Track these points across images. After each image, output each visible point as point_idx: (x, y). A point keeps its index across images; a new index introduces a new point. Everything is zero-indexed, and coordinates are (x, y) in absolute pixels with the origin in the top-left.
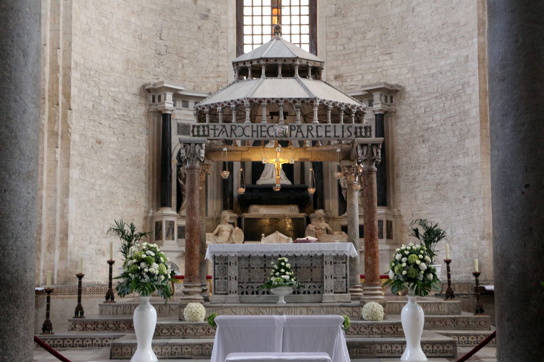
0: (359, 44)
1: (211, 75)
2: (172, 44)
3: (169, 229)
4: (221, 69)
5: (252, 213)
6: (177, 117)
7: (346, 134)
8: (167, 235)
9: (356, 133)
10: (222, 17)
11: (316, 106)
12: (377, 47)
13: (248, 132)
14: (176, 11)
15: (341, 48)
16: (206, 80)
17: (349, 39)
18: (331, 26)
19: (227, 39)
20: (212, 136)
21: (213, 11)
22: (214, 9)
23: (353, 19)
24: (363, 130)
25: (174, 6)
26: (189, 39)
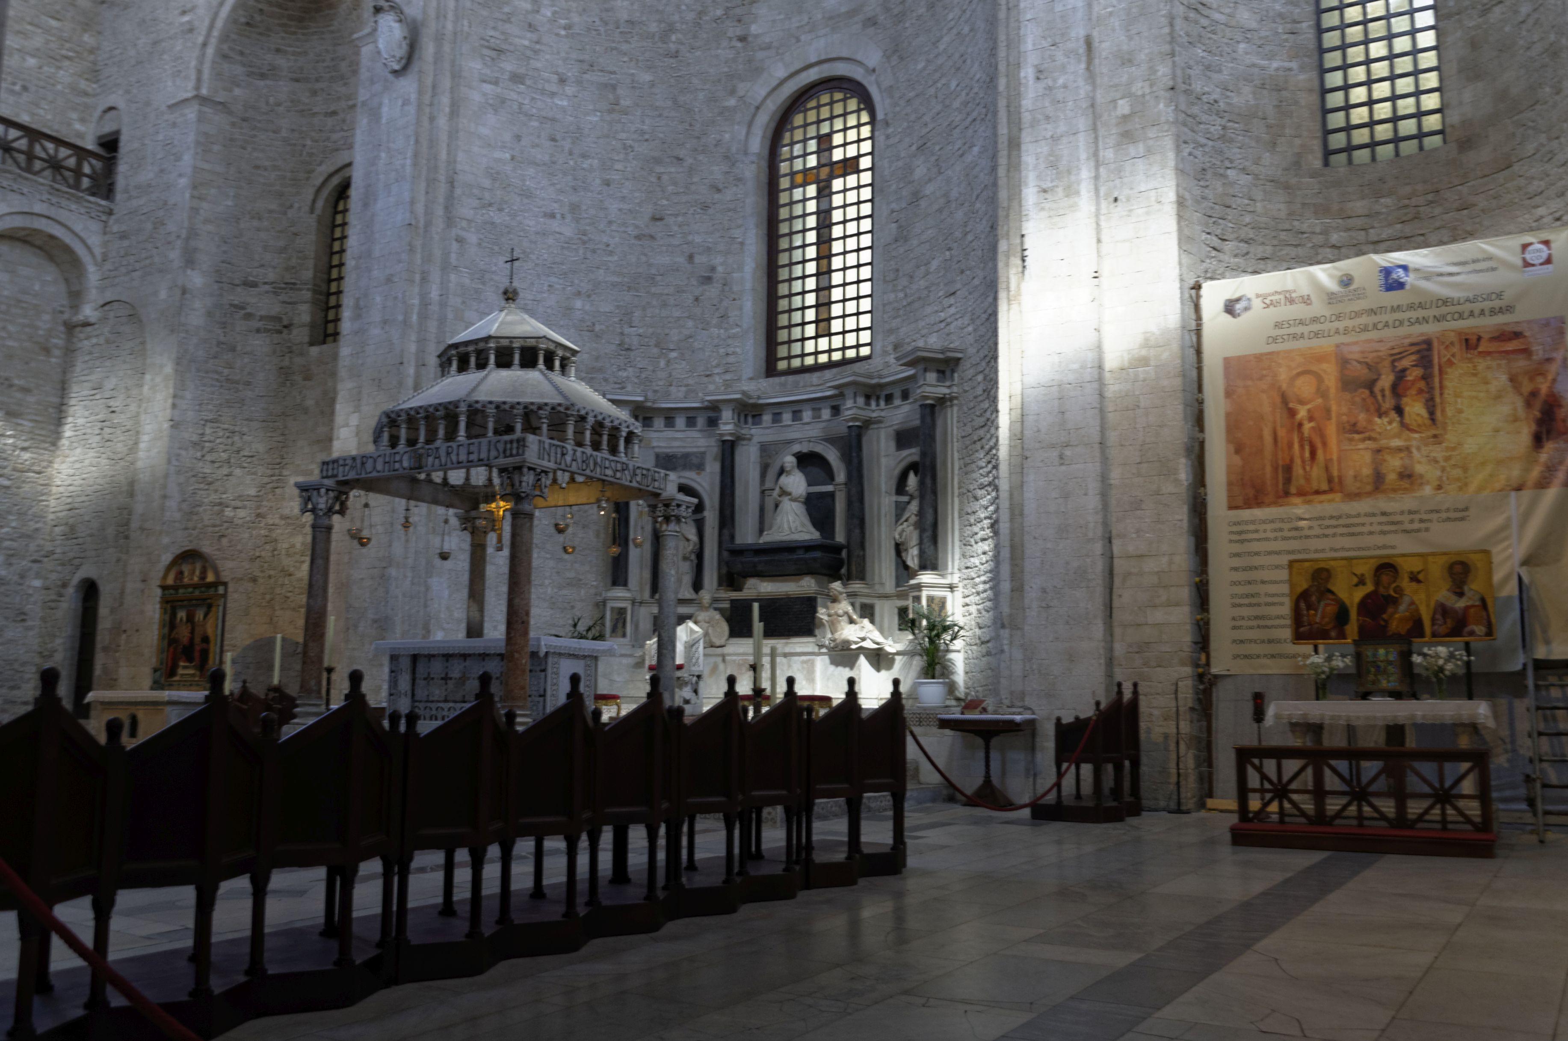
0: (923, 283)
1: (716, 371)
2: (651, 330)
3: (617, 620)
4: (731, 359)
5: (745, 591)
6: (655, 444)
7: (493, 453)
8: (614, 630)
9: (505, 451)
11: (461, 413)
13: (379, 466)
14: (659, 278)
16: (706, 379)
17: (911, 277)
20: (341, 478)
21: (720, 269)
22: (722, 264)
24: (515, 445)
25: (653, 271)
26: (679, 318)
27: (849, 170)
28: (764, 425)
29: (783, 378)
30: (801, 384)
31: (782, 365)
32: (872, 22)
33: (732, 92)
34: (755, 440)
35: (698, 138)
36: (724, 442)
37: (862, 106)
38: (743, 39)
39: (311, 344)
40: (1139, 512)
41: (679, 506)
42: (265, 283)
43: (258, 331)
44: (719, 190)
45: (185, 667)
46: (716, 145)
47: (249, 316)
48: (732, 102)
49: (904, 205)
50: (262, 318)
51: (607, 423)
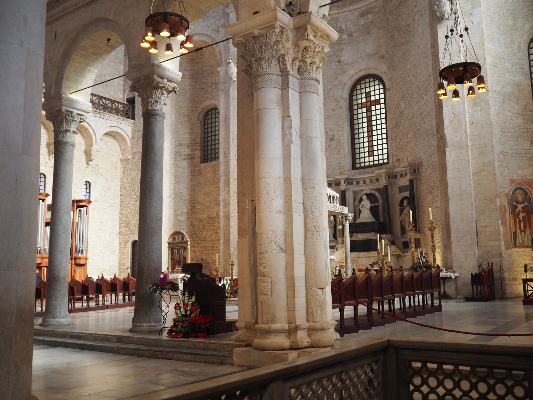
1: (337, 168)
4: (341, 165)
10: (341, 137)
12: (412, 142)
15: (398, 144)
16: (334, 171)
17: (401, 139)
18: (393, 133)
19: (344, 148)
21: (336, 136)
23: (402, 128)
27: (377, 103)
28: (354, 185)
29: (359, 170)
30: (365, 172)
31: (358, 166)
32: (382, 57)
33: (337, 79)
34: (351, 190)
35: (326, 94)
36: (342, 191)
37: (380, 83)
38: (339, 62)
39: (201, 163)
40: (484, 214)
41: (349, 216)
42: (185, 144)
43: (184, 159)
44: (334, 111)
45: (177, 267)
46: (332, 96)
47: (181, 155)
48: (337, 82)
49: (397, 116)
50: (185, 155)
51: (332, 196)
